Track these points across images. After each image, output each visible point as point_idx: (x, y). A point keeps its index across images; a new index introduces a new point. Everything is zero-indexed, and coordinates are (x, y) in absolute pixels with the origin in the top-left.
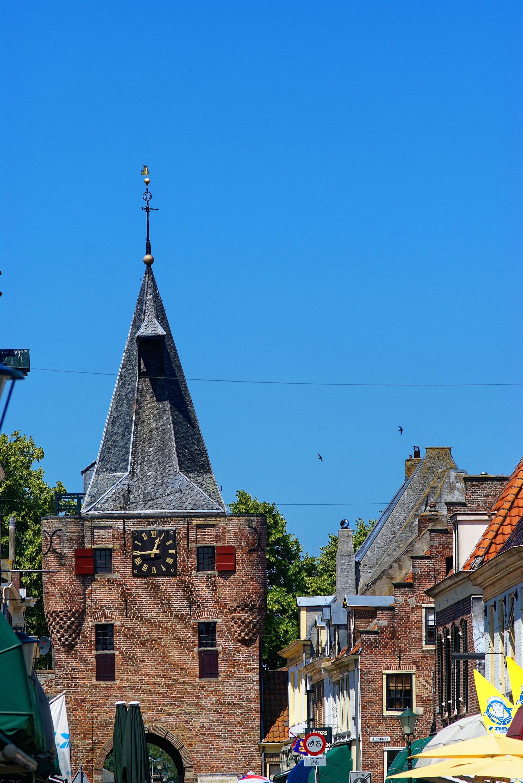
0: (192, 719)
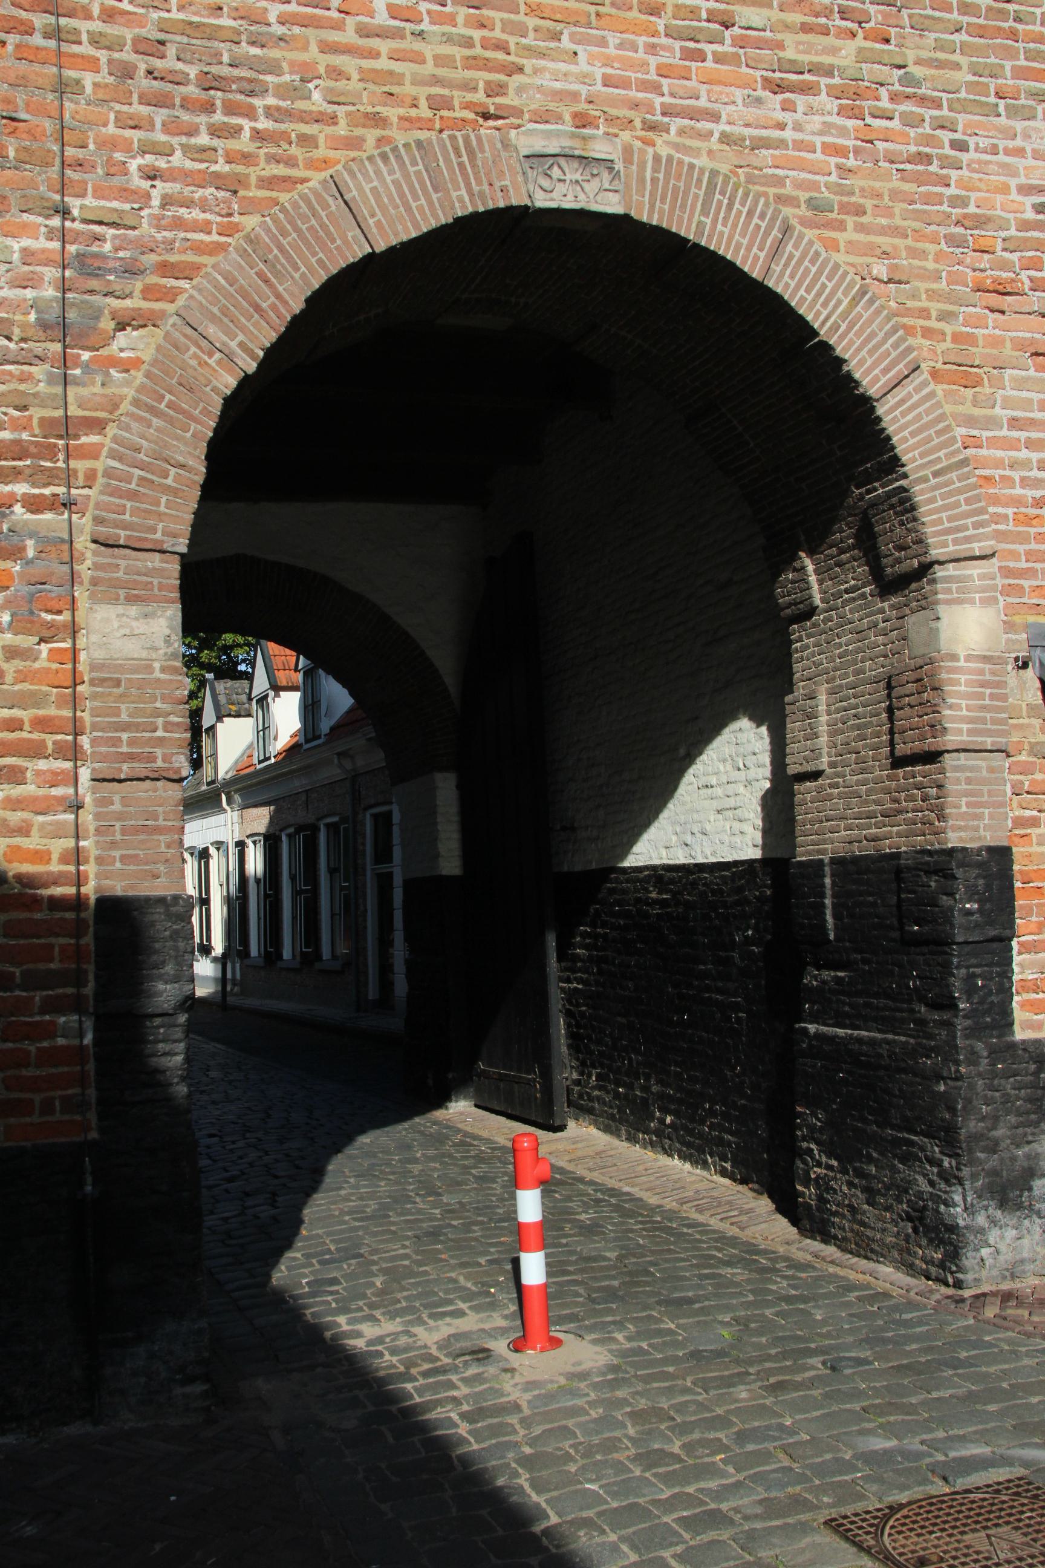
0: (960, 146)
